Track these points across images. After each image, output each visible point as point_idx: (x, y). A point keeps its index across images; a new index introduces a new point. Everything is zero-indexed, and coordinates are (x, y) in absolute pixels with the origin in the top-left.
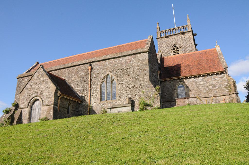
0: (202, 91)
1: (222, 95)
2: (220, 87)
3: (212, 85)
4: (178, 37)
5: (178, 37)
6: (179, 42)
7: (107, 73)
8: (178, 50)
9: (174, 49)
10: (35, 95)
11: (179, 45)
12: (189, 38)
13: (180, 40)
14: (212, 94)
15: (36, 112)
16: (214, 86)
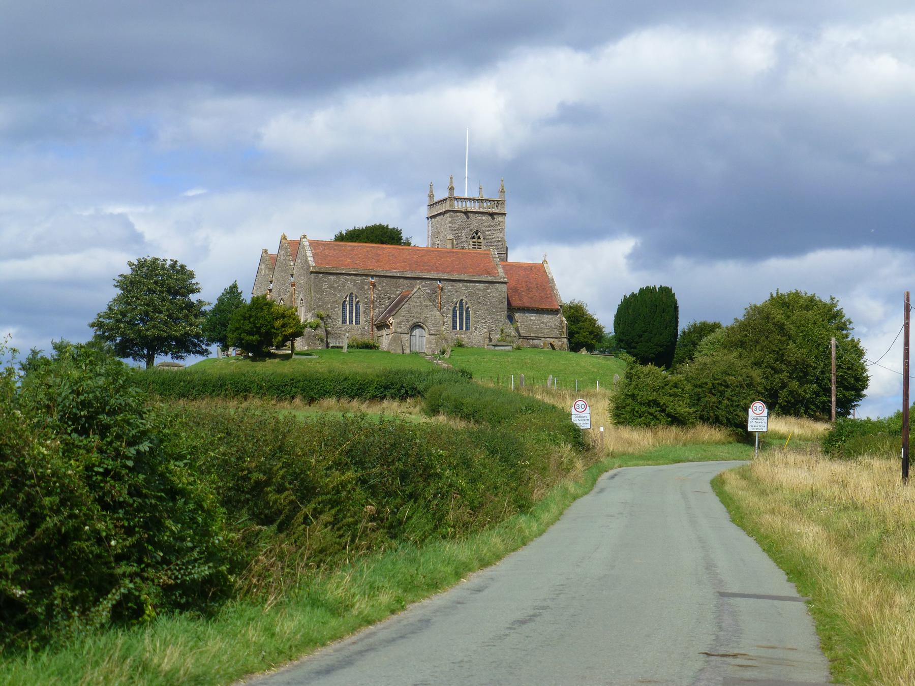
0: (532, 327)
1: (551, 336)
2: (551, 327)
3: (543, 323)
4: (483, 218)
5: (483, 218)
6: (483, 228)
7: (461, 298)
8: (479, 241)
9: (473, 238)
10: (417, 320)
11: (483, 233)
12: (499, 224)
13: (485, 224)
14: (542, 333)
15: (416, 339)
16: (546, 324)
